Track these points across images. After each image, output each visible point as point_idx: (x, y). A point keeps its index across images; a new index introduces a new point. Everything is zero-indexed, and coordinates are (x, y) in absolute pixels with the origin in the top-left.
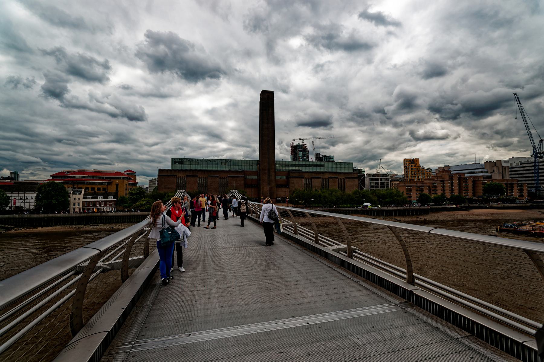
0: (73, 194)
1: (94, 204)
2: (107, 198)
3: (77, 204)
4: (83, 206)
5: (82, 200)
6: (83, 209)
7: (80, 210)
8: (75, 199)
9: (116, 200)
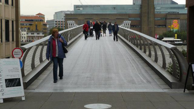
0: (22, 31)
1: (33, 37)
2: (39, 34)
3: (24, 38)
4: (27, 39)
5: (26, 35)
6: (27, 41)
7: (25, 41)
8: (23, 34)
9: (44, 35)
